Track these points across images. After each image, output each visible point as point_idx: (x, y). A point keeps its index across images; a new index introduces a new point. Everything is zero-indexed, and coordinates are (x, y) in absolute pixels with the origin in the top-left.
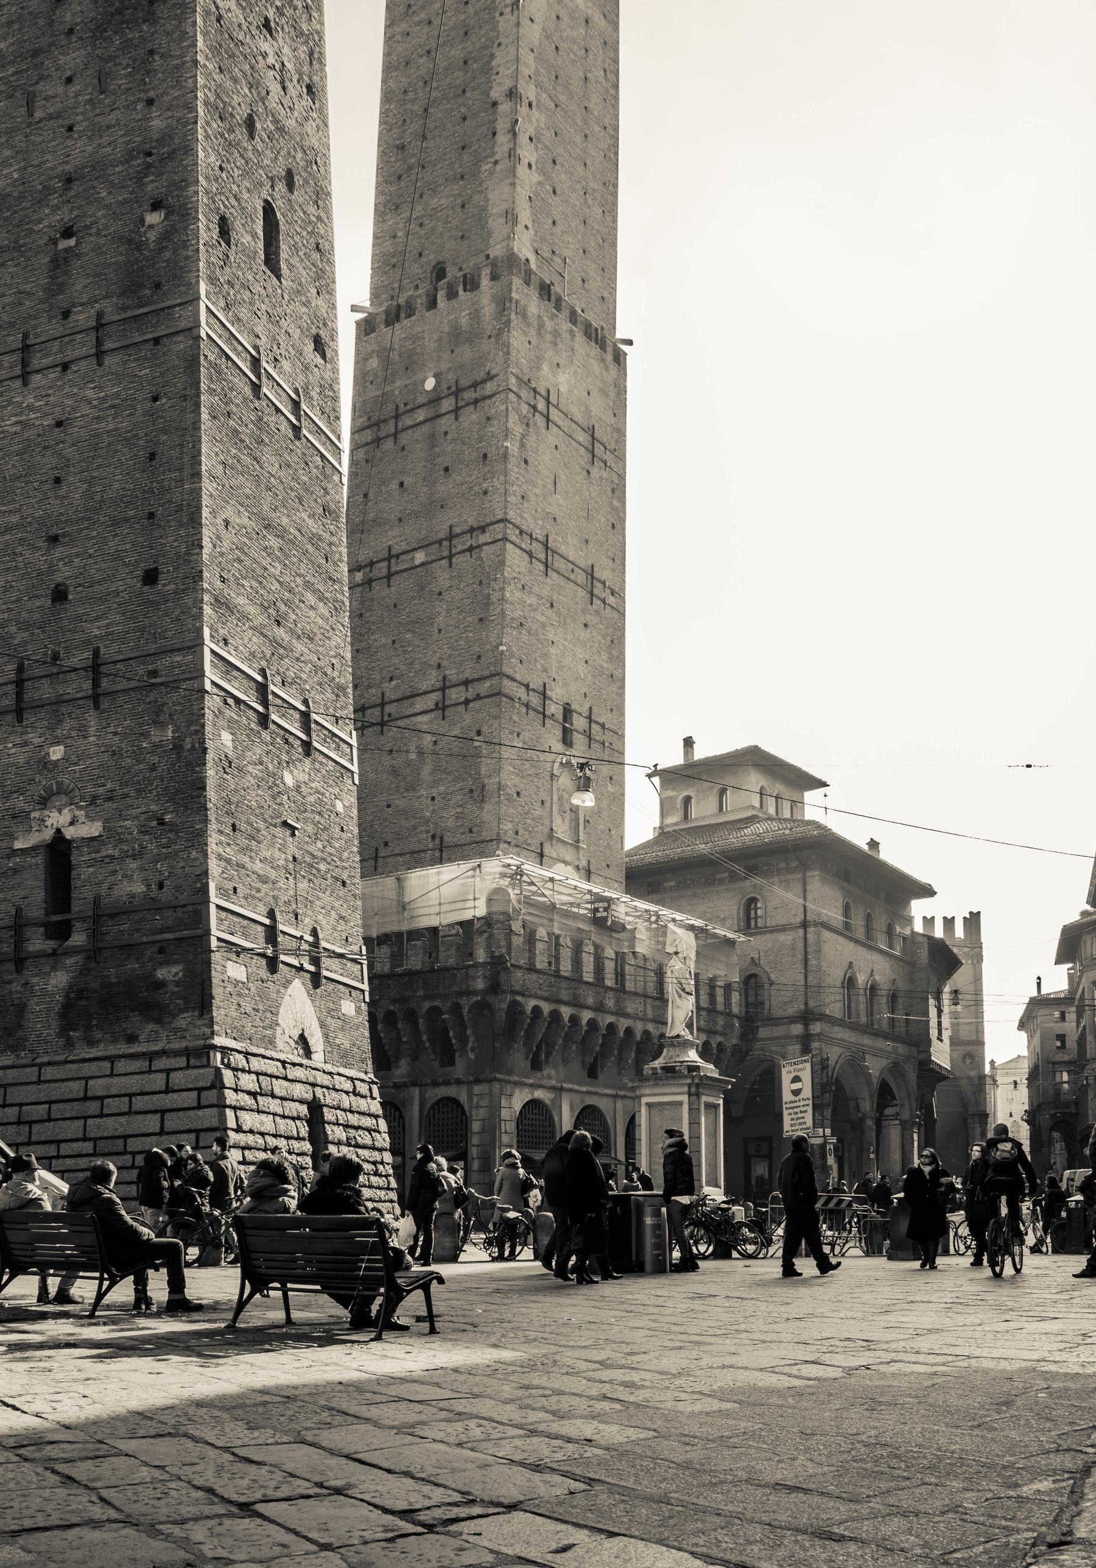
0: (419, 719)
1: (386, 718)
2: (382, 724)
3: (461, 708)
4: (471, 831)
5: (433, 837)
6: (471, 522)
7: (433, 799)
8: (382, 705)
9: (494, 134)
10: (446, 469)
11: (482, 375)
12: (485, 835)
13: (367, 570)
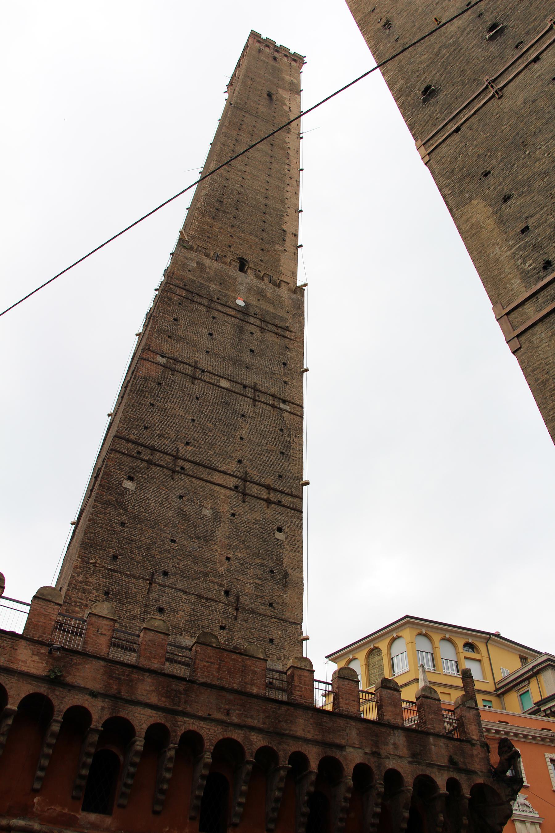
0: (217, 488)
1: (178, 469)
2: (174, 472)
3: (265, 504)
4: (271, 605)
5: (227, 593)
6: (273, 391)
7: (228, 559)
8: (176, 458)
9: (284, 240)
10: (252, 351)
11: (282, 324)
12: (288, 615)
13: (172, 361)
